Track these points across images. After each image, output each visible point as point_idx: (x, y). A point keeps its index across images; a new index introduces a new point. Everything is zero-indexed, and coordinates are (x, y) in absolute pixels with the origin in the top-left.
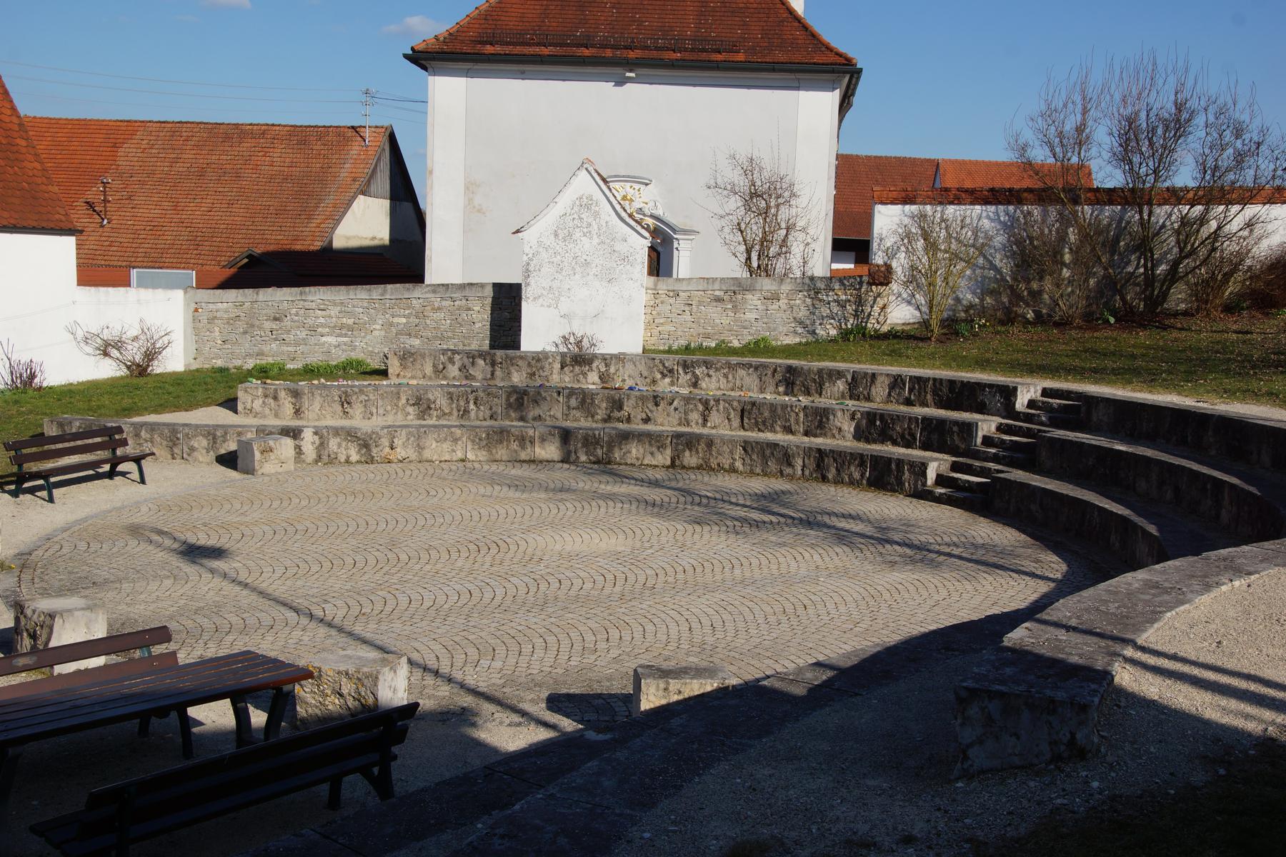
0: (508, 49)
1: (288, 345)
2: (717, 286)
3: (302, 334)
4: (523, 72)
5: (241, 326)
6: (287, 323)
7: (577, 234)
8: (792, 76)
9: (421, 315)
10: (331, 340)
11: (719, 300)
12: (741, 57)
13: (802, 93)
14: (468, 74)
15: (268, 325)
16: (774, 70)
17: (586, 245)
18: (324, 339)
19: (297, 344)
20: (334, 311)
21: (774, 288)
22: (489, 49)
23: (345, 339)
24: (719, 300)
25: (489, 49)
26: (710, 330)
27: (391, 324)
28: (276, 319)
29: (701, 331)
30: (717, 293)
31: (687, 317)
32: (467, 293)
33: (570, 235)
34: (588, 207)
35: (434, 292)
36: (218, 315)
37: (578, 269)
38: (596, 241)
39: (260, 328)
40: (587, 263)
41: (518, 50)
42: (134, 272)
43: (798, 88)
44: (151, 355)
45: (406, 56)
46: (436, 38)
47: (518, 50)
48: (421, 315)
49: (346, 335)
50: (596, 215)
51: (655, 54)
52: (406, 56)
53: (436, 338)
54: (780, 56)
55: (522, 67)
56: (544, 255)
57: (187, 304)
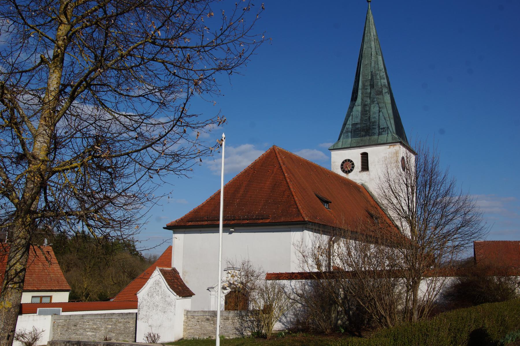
0: (197, 223)
1: (78, 335)
2: (207, 314)
3: (82, 331)
4: (200, 231)
5: (65, 328)
6: (78, 327)
7: (155, 295)
8: (287, 227)
9: (115, 324)
10: (90, 333)
11: (208, 319)
12: (268, 221)
13: (292, 233)
14: (184, 233)
15: (73, 328)
16: (277, 225)
17: (157, 298)
18: (88, 333)
19: (80, 335)
20: (91, 323)
21: (227, 315)
22: (190, 223)
23: (94, 333)
24: (208, 319)
25: (190, 223)
26: (206, 332)
27: (107, 328)
28: (75, 326)
29: (203, 332)
30: (208, 317)
31: (198, 327)
32: (129, 316)
33: (152, 295)
34: (158, 284)
35: (119, 316)
36: (60, 324)
37: (155, 308)
38: (160, 297)
39: (71, 329)
40: (157, 306)
41: (200, 223)
42: (38, 309)
43: (290, 231)
44: (35, 339)
45: (164, 228)
46: (176, 221)
47: (200, 223)
48: (115, 324)
49: (94, 332)
50: (160, 287)
51: (239, 222)
52: (164, 228)
53: (119, 333)
54: (283, 219)
55: (184, 230)
56: (144, 303)
57: (52, 321)
